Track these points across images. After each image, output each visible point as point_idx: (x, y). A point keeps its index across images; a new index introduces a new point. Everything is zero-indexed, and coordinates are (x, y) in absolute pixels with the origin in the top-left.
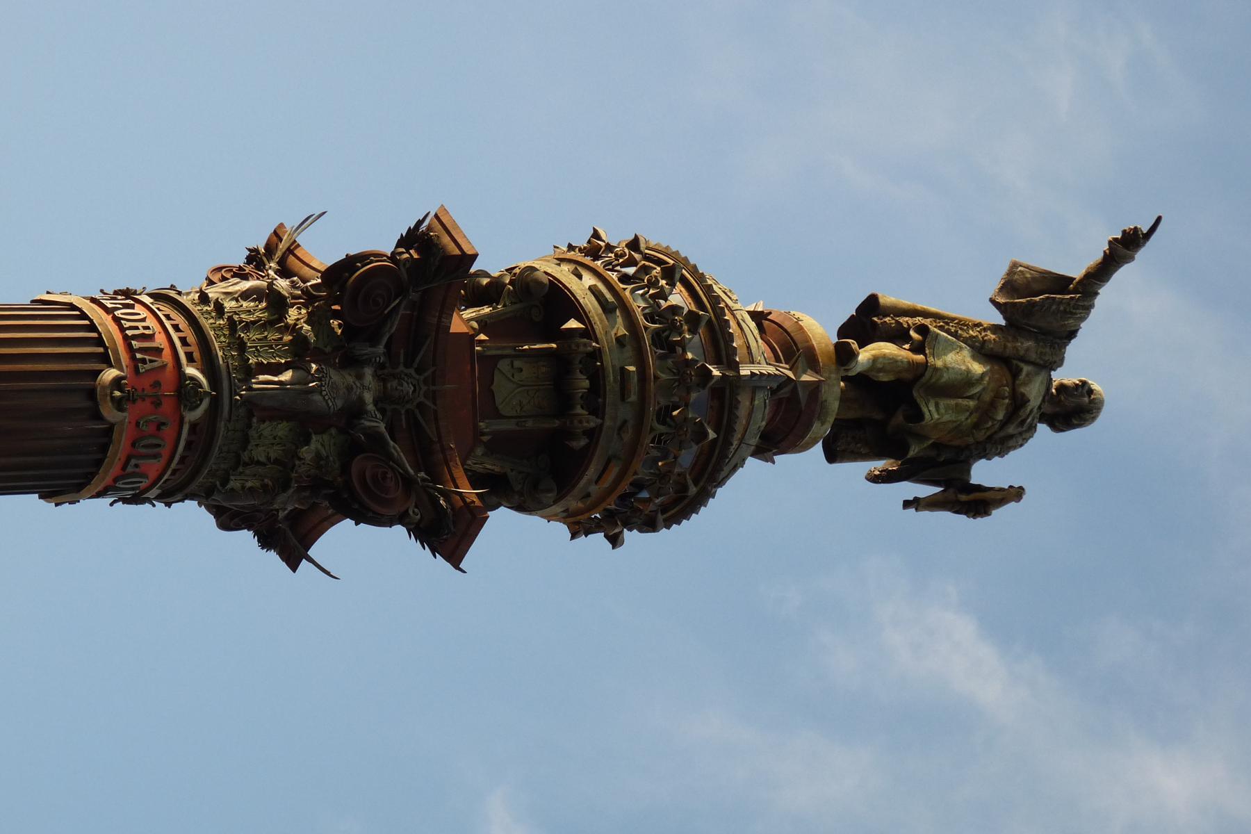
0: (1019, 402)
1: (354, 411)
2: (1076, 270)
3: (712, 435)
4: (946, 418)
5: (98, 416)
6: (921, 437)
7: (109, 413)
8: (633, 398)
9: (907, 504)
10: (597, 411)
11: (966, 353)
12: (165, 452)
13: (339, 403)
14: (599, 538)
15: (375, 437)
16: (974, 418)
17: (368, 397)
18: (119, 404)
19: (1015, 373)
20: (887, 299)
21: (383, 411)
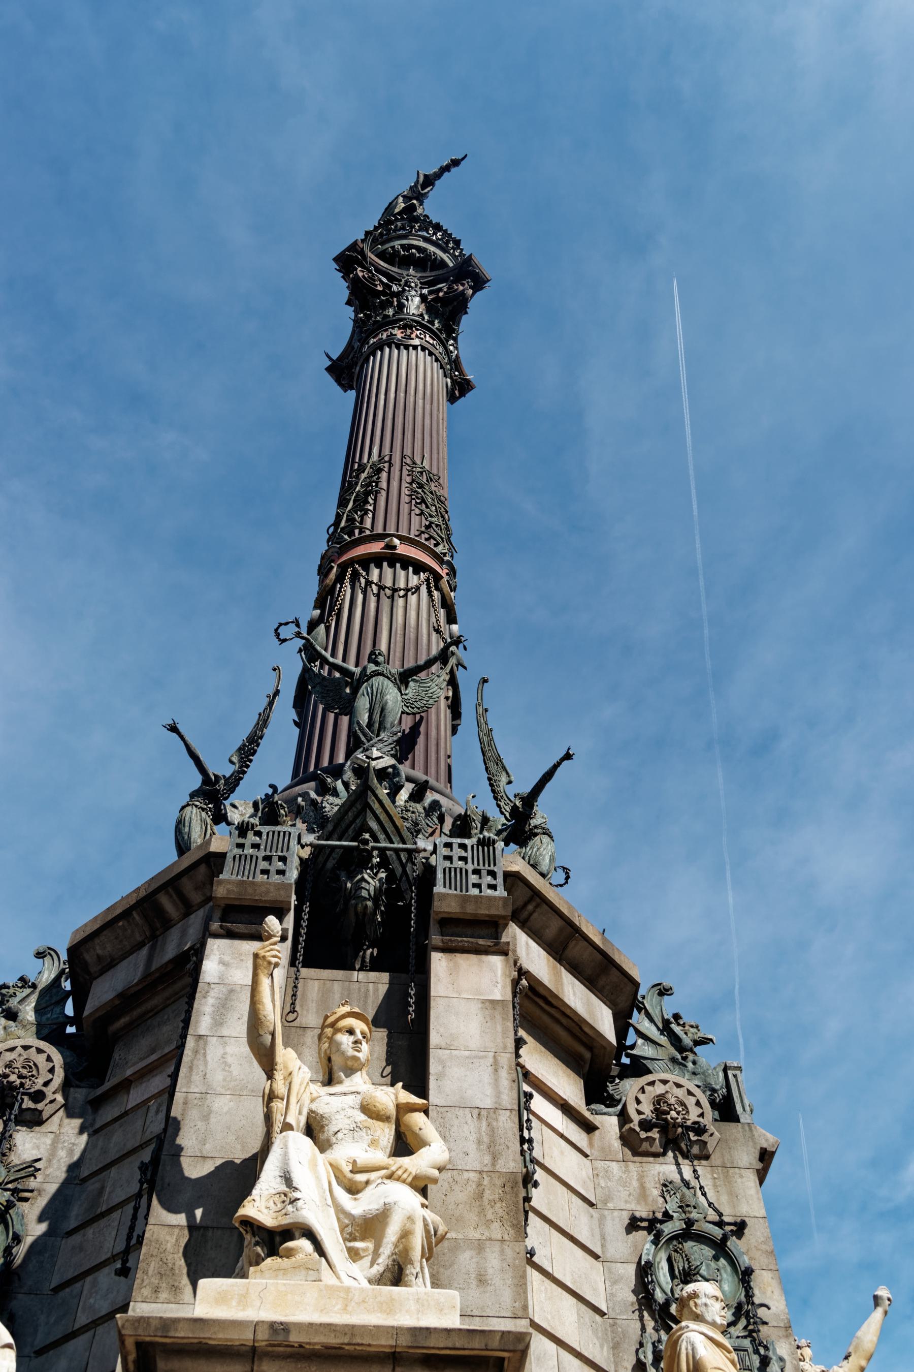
5: (415, 347)
15: (430, 293)
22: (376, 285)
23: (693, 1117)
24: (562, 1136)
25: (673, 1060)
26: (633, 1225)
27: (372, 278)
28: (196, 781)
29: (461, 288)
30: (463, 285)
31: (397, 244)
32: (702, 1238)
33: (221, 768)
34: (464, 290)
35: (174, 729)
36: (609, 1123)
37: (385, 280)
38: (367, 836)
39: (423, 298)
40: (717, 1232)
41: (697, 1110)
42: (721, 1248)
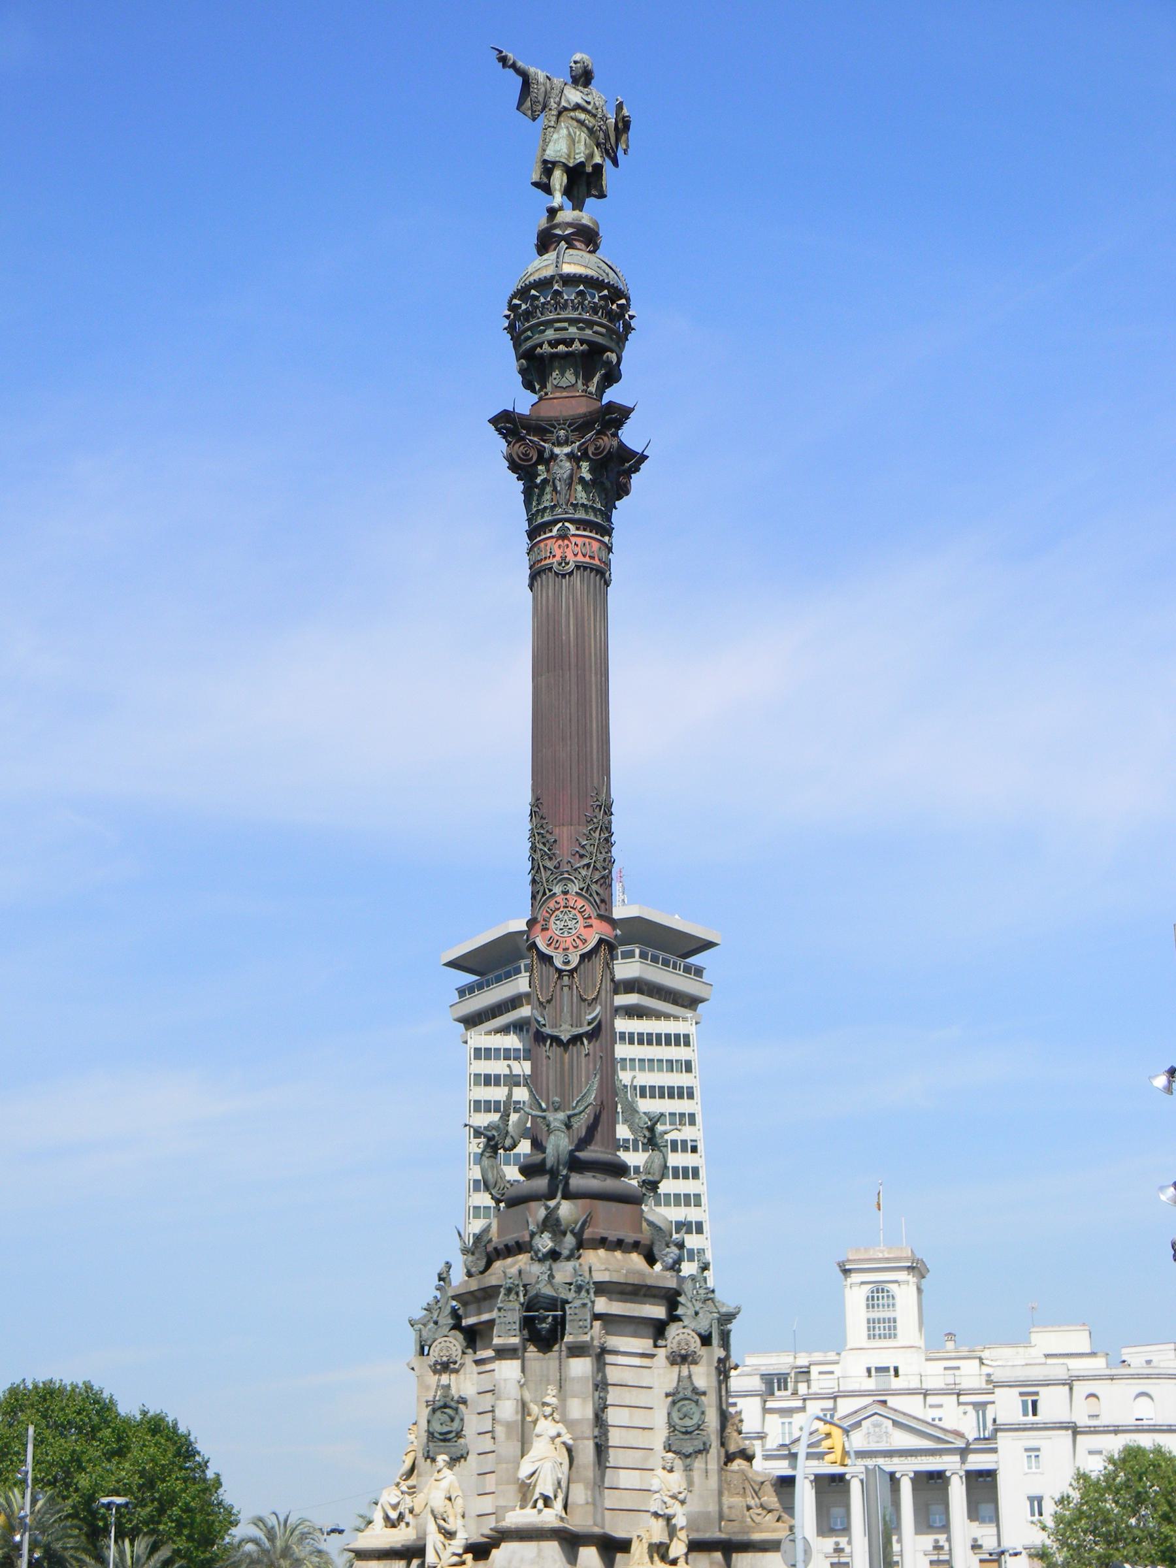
0: (578, 107)
1: (570, 456)
2: (520, 79)
3: (582, 287)
4: (582, 148)
6: (591, 156)
7: (571, 566)
8: (566, 325)
9: (625, 151)
10: (572, 341)
11: (555, 136)
12: (587, 540)
13: (568, 464)
14: (633, 323)
16: (585, 129)
17: (567, 450)
18: (567, 564)
19: (566, 109)
20: (535, 177)
21: (573, 442)
23: (692, 1349)
26: (667, 1395)
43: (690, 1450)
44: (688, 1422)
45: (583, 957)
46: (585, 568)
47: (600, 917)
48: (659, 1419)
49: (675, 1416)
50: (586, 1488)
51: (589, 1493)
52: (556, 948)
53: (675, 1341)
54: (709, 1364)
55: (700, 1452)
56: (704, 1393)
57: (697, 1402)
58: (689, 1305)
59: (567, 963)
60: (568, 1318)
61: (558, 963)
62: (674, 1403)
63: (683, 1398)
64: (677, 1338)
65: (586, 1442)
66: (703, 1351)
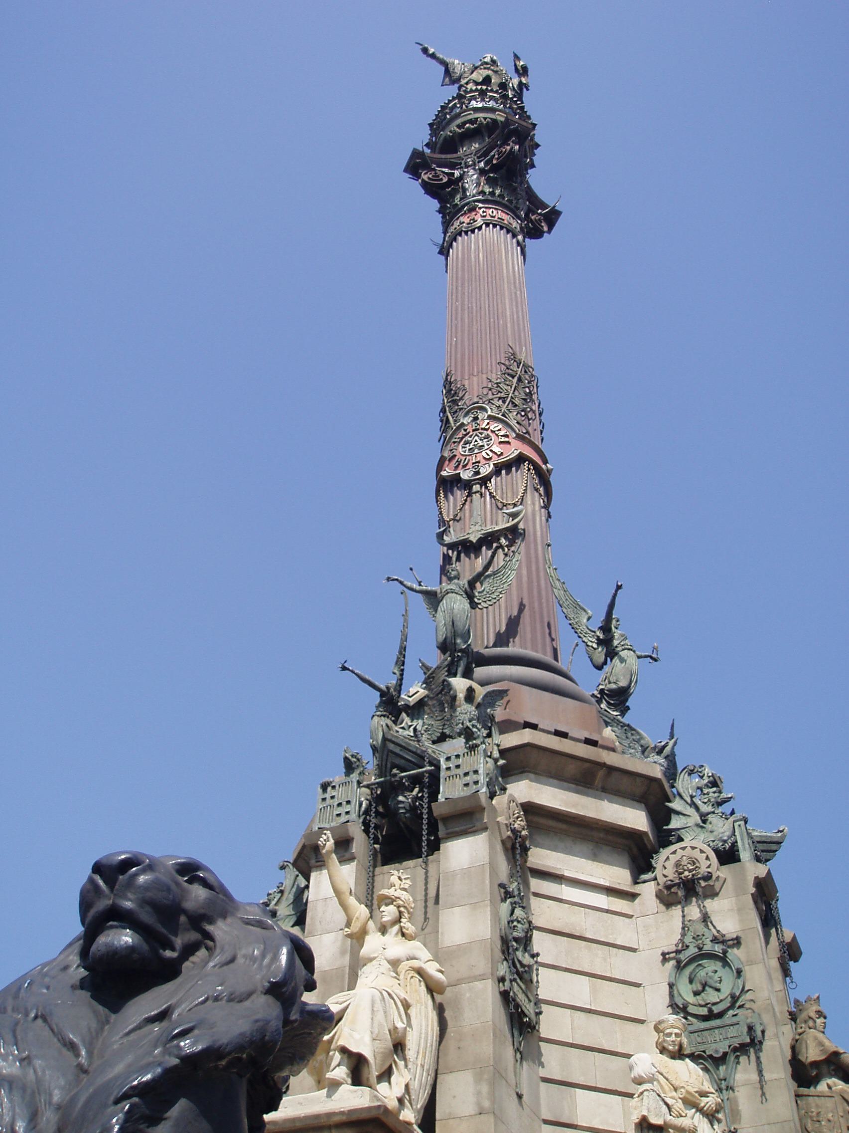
5: (480, 228)
15: (486, 164)
22: (442, 179)
23: (703, 870)
24: (607, 911)
25: (698, 825)
27: (436, 176)
28: (376, 697)
29: (508, 148)
30: (508, 145)
31: (453, 127)
32: (711, 956)
33: (387, 680)
34: (512, 148)
35: (344, 668)
36: (648, 890)
37: (446, 170)
38: (395, 771)
39: (482, 172)
40: (718, 949)
41: (708, 863)
42: (723, 960)
43: (723, 1047)
44: (711, 996)
45: (498, 470)
46: (495, 226)
47: (519, 437)
48: (654, 1003)
49: (686, 992)
50: (478, 1079)
51: (485, 1089)
52: (464, 466)
53: (670, 865)
54: (739, 890)
55: (741, 1049)
56: (737, 942)
57: (723, 960)
58: (691, 811)
59: (477, 473)
60: (443, 774)
61: (466, 475)
62: (680, 967)
63: (694, 957)
64: (673, 859)
65: (478, 985)
66: (724, 872)
